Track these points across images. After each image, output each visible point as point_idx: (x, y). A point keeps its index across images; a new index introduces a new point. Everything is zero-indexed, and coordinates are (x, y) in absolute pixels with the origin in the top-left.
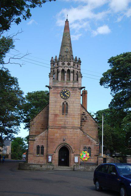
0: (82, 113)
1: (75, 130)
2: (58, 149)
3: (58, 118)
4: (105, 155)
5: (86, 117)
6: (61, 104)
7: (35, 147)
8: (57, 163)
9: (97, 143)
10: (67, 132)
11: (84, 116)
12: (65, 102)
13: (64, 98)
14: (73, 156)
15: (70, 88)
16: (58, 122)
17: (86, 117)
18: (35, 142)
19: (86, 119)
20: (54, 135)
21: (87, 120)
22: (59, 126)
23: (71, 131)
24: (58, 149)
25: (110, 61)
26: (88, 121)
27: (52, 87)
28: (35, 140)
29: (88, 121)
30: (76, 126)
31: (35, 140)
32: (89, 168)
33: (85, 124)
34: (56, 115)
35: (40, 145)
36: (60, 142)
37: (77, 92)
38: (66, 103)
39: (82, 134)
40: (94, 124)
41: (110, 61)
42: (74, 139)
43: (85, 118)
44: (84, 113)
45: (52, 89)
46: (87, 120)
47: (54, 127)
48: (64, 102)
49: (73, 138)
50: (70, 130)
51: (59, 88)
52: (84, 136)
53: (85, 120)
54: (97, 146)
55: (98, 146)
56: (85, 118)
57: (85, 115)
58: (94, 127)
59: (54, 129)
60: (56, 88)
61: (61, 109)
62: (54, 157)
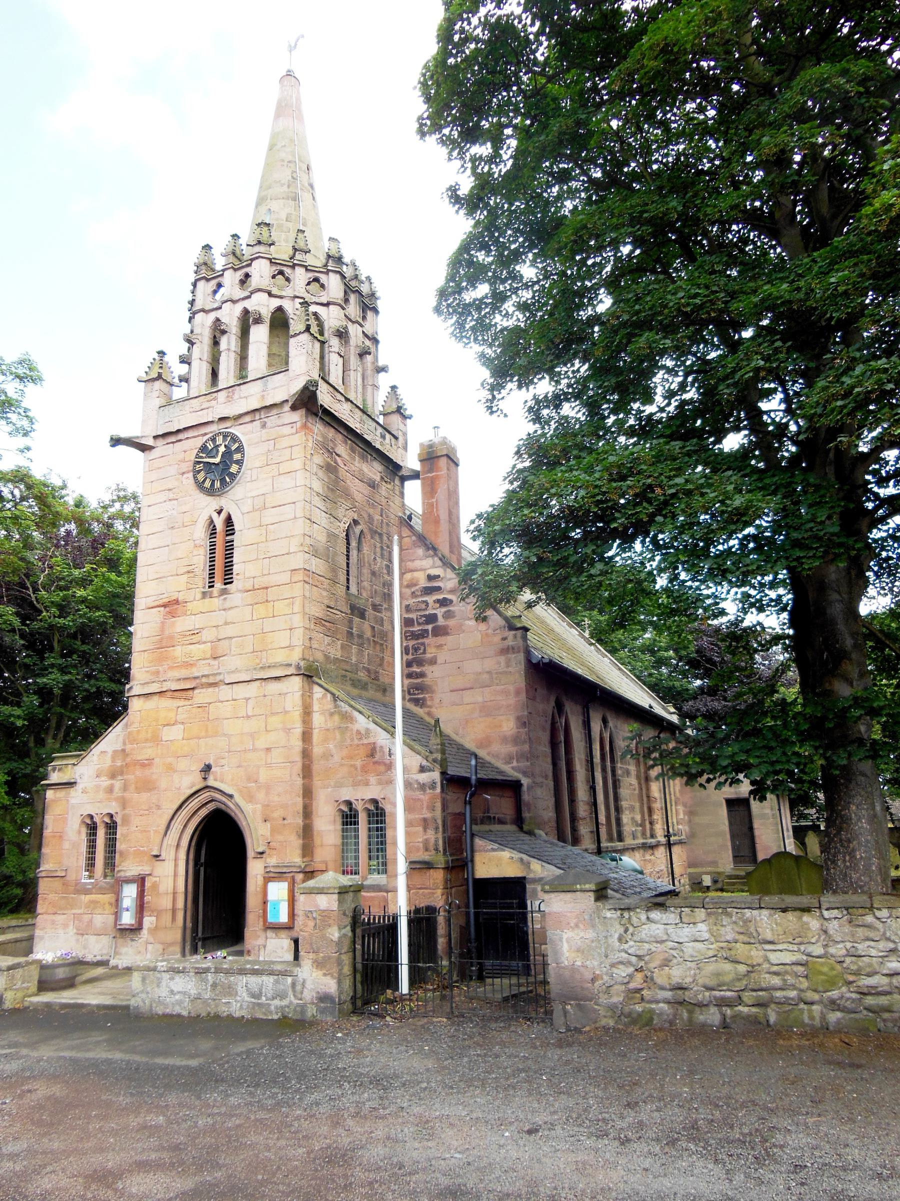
0: (423, 583)
1: (274, 687)
2: (177, 825)
3: (183, 624)
4: (517, 855)
5: (444, 603)
6: (200, 533)
7: (76, 835)
8: (176, 935)
9: (422, 769)
10: (225, 710)
11: (430, 599)
12: (219, 512)
13: (211, 492)
14: (260, 881)
15: (247, 419)
16: (178, 649)
17: (444, 603)
18: (75, 796)
19: (448, 615)
20: (156, 739)
21: (451, 623)
22: (184, 673)
23: (247, 699)
24: (177, 825)
25: (422, 134)
26: (460, 629)
27: (150, 442)
28: (71, 784)
29: (460, 629)
30: (280, 657)
31: (71, 784)
32: (230, 990)
33: (440, 647)
34: (172, 606)
35: (100, 809)
36: (189, 781)
37: (287, 430)
38: (223, 515)
39: (322, 713)
40: (497, 639)
41: (422, 134)
42: (268, 750)
43: (440, 612)
44: (430, 578)
45: (154, 454)
46: (451, 623)
47: (155, 688)
48: (215, 516)
49: (261, 743)
50: (241, 691)
51: (190, 434)
52: (336, 718)
53: (441, 621)
54: (422, 787)
55: (433, 786)
56: (440, 612)
57: (438, 589)
58: (502, 659)
59: (156, 698)
60: (173, 439)
61: (200, 560)
62: (155, 886)
